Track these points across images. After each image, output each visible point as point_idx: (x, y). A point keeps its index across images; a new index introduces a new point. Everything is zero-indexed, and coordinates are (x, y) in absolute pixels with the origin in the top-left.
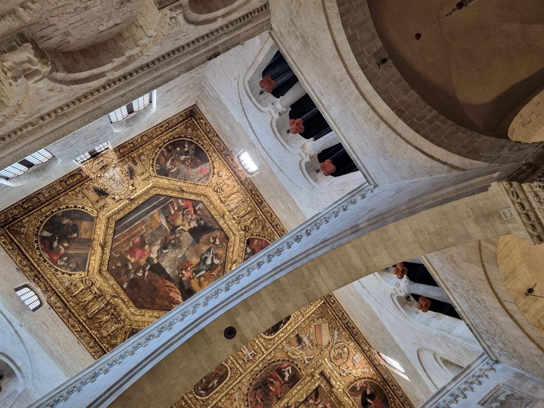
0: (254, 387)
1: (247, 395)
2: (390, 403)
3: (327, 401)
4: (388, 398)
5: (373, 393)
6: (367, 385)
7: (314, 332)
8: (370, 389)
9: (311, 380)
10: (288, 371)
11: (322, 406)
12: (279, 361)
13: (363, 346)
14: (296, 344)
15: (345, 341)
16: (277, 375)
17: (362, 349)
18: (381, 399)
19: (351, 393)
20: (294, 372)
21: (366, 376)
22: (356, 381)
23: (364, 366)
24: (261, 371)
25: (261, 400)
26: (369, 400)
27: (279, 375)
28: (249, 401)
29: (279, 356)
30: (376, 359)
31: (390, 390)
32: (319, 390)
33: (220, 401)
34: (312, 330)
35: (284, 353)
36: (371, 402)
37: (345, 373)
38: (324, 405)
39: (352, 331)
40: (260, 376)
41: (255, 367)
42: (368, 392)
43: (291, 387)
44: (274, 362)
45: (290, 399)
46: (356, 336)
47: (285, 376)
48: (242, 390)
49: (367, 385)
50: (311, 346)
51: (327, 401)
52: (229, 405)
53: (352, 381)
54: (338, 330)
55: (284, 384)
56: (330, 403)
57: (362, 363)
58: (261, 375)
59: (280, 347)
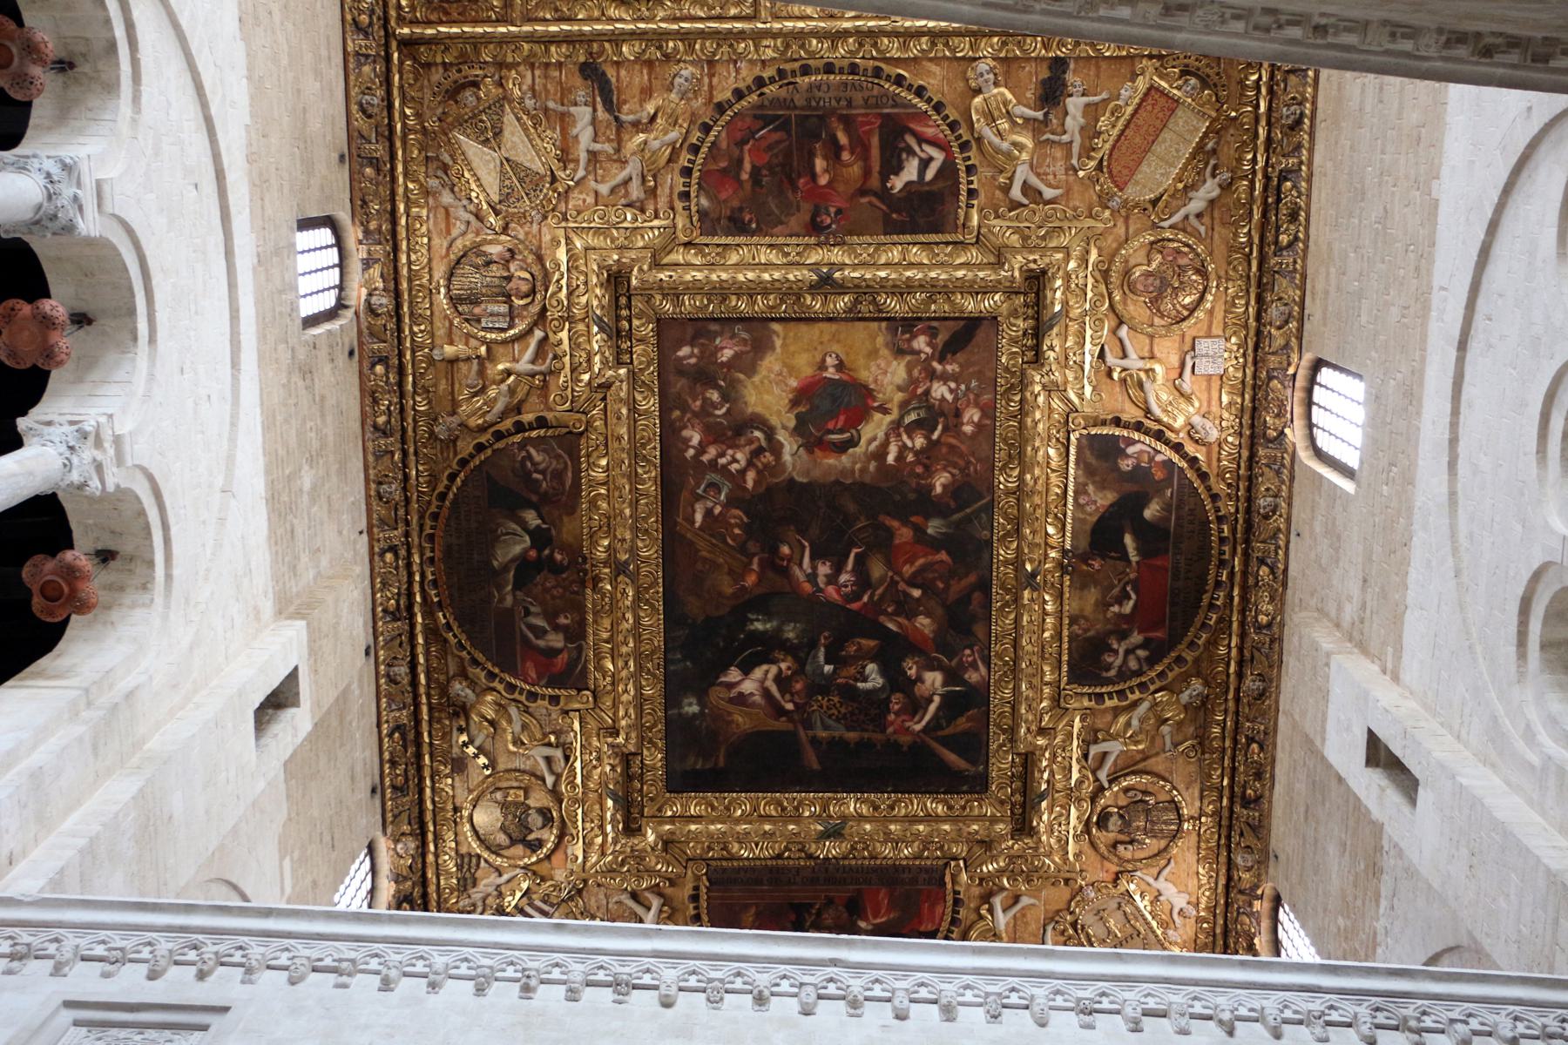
0: (762, 107)
1: (721, 108)
2: (1198, 621)
3: (977, 396)
4: (1206, 598)
5: (1167, 531)
6: (1168, 481)
7: (1130, 110)
8: (1167, 508)
9: (981, 267)
10: (925, 163)
11: (949, 397)
12: (920, 92)
13: (1274, 312)
14: (1029, 95)
15: (1220, 249)
16: (875, 141)
17: (1258, 333)
18: (1176, 577)
19: (1088, 453)
20: (941, 184)
21: (1190, 449)
22: (1138, 427)
23: (1215, 408)
24: (829, 69)
25: (755, 173)
26: (1128, 540)
27: (882, 148)
28: (711, 138)
29: (935, 79)
30: (1281, 406)
31: (1238, 578)
32: (980, 335)
33: (617, 39)
34: (1130, 93)
35: (961, 85)
36: (1133, 556)
37: (1125, 363)
38: (956, 399)
39: (1278, 228)
40: (811, 85)
41: (820, 35)
42: (1151, 512)
43: (892, 228)
44: (899, 80)
45: (855, 267)
46: (1279, 249)
47: (898, 169)
48: (715, 80)
49: (1168, 481)
50: (1076, 148)
51: (977, 396)
52: (636, 91)
53: (1125, 417)
54: (1226, 187)
55: (876, 194)
56: (984, 415)
57: (1215, 394)
58: (819, 88)
59: (964, 48)
